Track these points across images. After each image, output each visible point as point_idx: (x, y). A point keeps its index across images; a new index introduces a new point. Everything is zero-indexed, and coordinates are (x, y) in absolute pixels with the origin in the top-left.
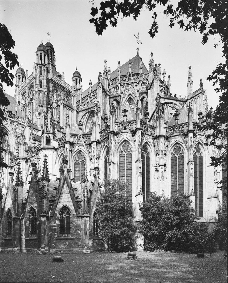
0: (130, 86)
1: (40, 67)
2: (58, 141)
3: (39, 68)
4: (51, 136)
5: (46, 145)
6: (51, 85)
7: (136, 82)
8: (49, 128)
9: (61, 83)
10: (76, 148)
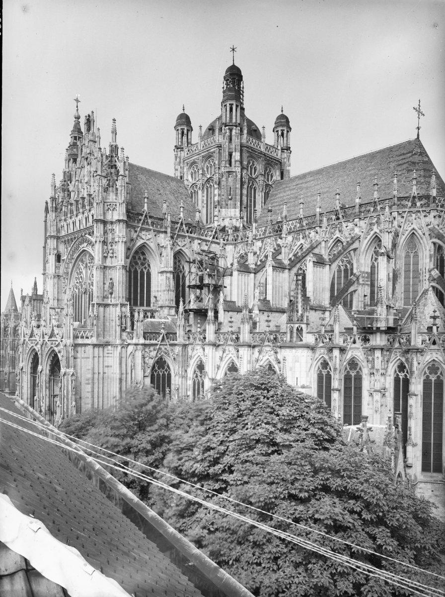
0: (414, 215)
1: (229, 129)
3: (228, 131)
4: (304, 326)
7: (425, 211)
9: (260, 147)
10: (349, 356)
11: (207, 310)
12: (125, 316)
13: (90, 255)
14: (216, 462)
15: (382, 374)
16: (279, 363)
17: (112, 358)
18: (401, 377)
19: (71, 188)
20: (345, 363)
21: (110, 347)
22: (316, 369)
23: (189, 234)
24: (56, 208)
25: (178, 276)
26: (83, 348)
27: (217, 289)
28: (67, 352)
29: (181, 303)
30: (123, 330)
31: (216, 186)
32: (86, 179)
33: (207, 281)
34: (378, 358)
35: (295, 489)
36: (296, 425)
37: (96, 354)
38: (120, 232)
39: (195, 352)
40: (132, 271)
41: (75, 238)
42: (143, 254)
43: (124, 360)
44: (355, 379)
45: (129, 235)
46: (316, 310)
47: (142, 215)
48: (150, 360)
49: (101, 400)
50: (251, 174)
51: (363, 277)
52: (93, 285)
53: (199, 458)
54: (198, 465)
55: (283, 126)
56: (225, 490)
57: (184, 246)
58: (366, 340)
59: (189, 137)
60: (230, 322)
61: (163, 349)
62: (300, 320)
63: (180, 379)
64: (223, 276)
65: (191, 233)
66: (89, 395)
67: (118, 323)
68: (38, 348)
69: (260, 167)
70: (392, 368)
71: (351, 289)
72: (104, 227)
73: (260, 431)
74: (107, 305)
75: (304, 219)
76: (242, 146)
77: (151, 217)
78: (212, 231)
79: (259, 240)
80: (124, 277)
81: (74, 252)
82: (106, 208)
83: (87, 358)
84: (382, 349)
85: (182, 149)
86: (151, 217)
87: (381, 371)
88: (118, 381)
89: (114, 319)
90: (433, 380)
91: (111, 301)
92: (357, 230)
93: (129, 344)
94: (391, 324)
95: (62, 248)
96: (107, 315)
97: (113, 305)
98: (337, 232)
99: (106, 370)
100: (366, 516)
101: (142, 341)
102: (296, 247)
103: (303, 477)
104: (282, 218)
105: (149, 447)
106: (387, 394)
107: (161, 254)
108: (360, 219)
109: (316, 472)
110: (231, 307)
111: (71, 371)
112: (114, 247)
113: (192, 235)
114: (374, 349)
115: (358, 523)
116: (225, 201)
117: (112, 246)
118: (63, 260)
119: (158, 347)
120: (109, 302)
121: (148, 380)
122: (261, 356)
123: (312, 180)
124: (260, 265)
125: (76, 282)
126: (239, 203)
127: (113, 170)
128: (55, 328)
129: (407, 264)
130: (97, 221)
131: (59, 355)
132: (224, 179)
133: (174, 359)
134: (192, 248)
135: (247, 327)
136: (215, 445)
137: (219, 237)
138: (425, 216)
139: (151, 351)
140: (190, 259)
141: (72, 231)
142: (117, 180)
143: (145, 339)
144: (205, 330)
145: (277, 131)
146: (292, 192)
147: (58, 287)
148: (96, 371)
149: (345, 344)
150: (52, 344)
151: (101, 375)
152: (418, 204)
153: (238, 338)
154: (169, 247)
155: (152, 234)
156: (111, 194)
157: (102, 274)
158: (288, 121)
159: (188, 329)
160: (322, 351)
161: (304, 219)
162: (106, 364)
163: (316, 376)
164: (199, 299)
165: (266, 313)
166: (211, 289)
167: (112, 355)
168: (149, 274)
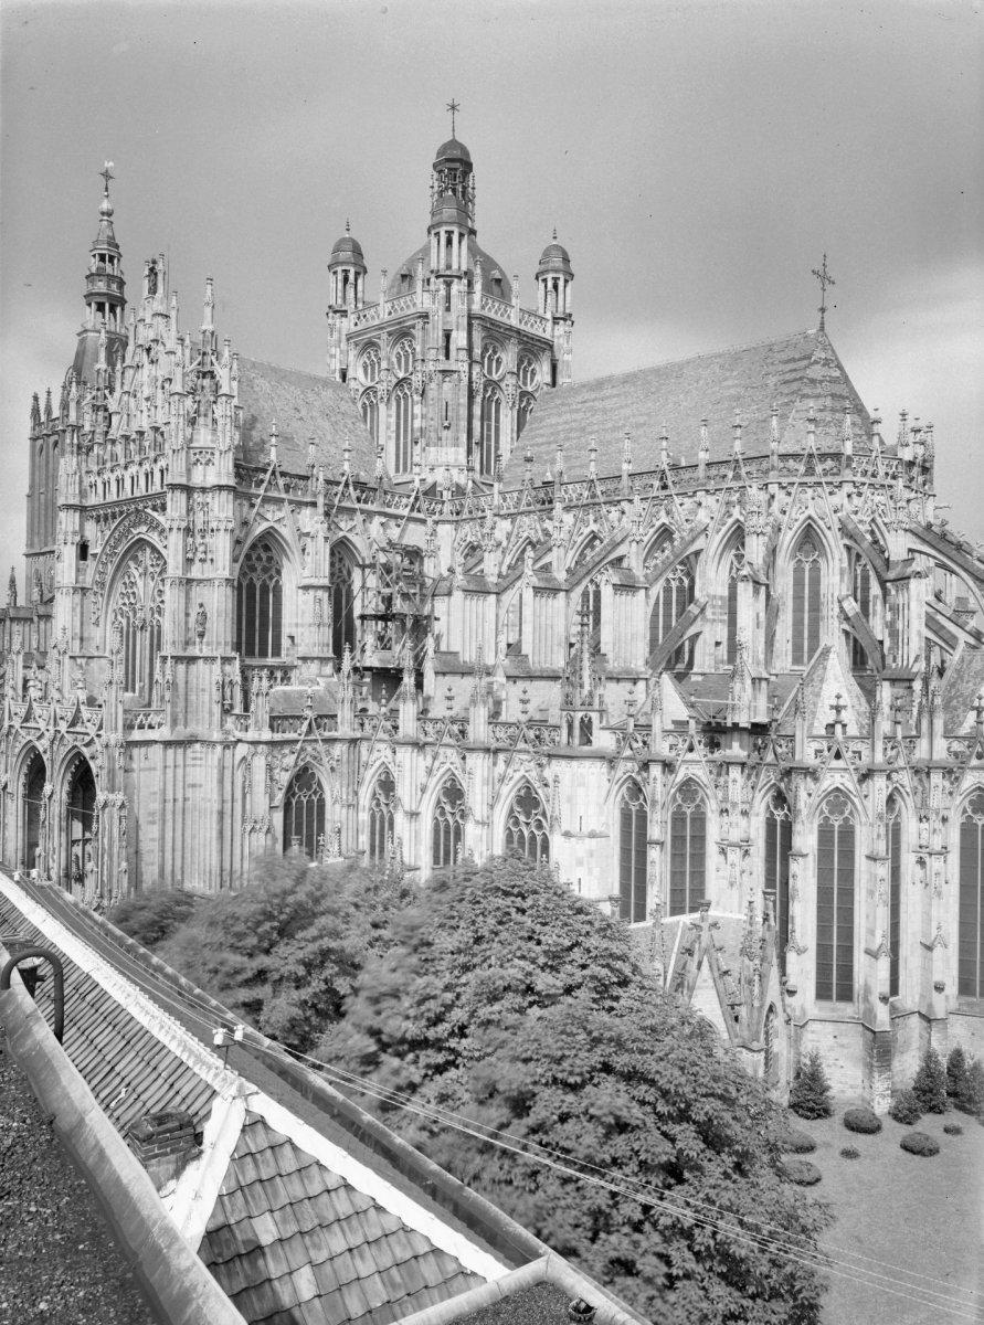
0: (810, 491)
3: (442, 287)
4: (595, 716)
6: (477, 336)
9: (509, 317)
11: (400, 671)
12: (231, 682)
13: (154, 549)
14: (437, 1020)
15: (745, 813)
16: (546, 785)
17: (203, 768)
18: (778, 819)
19: (113, 406)
20: (673, 791)
21: (198, 746)
22: (619, 798)
23: (362, 506)
24: (79, 447)
25: (340, 594)
26: (143, 750)
27: (420, 627)
28: (111, 759)
29: (347, 655)
30: (226, 711)
31: (417, 398)
32: (147, 392)
33: (399, 605)
34: (735, 781)
35: (563, 1071)
36: (567, 959)
37: (170, 762)
38: (222, 509)
39: (376, 754)
40: (244, 584)
41: (121, 513)
42: (267, 548)
43: (228, 773)
44: (693, 820)
45: (237, 514)
46: (618, 680)
47: (265, 471)
48: (283, 773)
49: (178, 854)
50: (490, 372)
51: (714, 607)
52: (159, 613)
53: (412, 1012)
54: (409, 1024)
55: (556, 271)
56: (453, 1064)
57: (350, 530)
58: (713, 745)
59: (360, 288)
60: (449, 698)
61: (309, 749)
62: (588, 704)
63: (344, 811)
64: (434, 595)
65: (366, 502)
66: (156, 846)
67: (217, 696)
68: (42, 745)
69: (509, 357)
70: (761, 804)
71: (691, 631)
72: (189, 498)
73: (512, 971)
74: (192, 660)
75: (597, 483)
76: (470, 317)
77: (283, 474)
78: (409, 497)
79: (504, 517)
80: (230, 601)
81: (119, 540)
82: (193, 459)
83: (150, 769)
84: (743, 765)
85: (344, 313)
86: (283, 474)
87: (741, 807)
88: (215, 817)
89: (207, 687)
90: (837, 824)
91: (201, 650)
92: (702, 516)
93: (239, 741)
94: (762, 719)
95: (91, 529)
96: (192, 678)
97: (206, 658)
98: (663, 513)
99: (189, 794)
100: (662, 1108)
101: (267, 735)
102: (581, 538)
103: (574, 1052)
104: (553, 476)
105: (301, 971)
106: (752, 850)
107: (304, 550)
108: (707, 491)
109: (597, 1041)
110: (452, 667)
111: (119, 797)
112: (207, 540)
113: (369, 507)
114: (729, 764)
115: (651, 1120)
116: (436, 431)
117: (203, 537)
118: (95, 555)
119: (298, 746)
120: (197, 653)
121: (278, 817)
122: (510, 771)
123: (618, 395)
124: (507, 576)
125: (121, 602)
126: (465, 436)
127: (207, 382)
128: (82, 708)
129: (798, 583)
130: (173, 487)
131: (92, 764)
132: (433, 385)
133: (332, 769)
134: (369, 536)
135: (480, 715)
136: (438, 992)
137: (425, 506)
138: (831, 493)
139: (284, 756)
140: (363, 559)
141: (115, 498)
142: (215, 402)
143: (273, 730)
144: (394, 712)
145: (545, 280)
146: (575, 416)
147: (82, 613)
148: (170, 796)
149: (674, 753)
150: (76, 740)
151: (180, 804)
152: (819, 469)
153: (463, 732)
154: (321, 536)
155: (287, 508)
156: (202, 431)
157: (183, 595)
158: (566, 260)
159: (360, 706)
160: (629, 765)
161: (597, 483)
162: (190, 780)
163: (617, 815)
164: (383, 642)
165: (519, 683)
166: (409, 624)
167: (203, 762)
168: (278, 590)
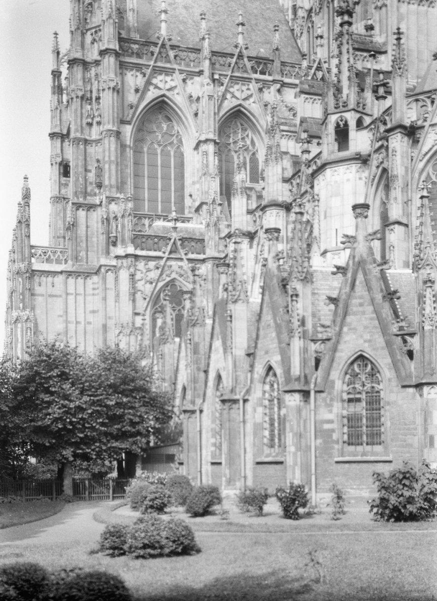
2: (371, 129)
4: (351, 118)
5: (339, 150)
8: (345, 91)
23: (258, 76)
26: (50, 279)
37: (71, 289)
48: (148, 285)
77: (173, 47)
86: (173, 47)
101: (131, 250)
107: (196, 115)
113: (266, 77)
119: (162, 262)
139: (149, 270)
151: (81, 327)
168: (180, 157)
